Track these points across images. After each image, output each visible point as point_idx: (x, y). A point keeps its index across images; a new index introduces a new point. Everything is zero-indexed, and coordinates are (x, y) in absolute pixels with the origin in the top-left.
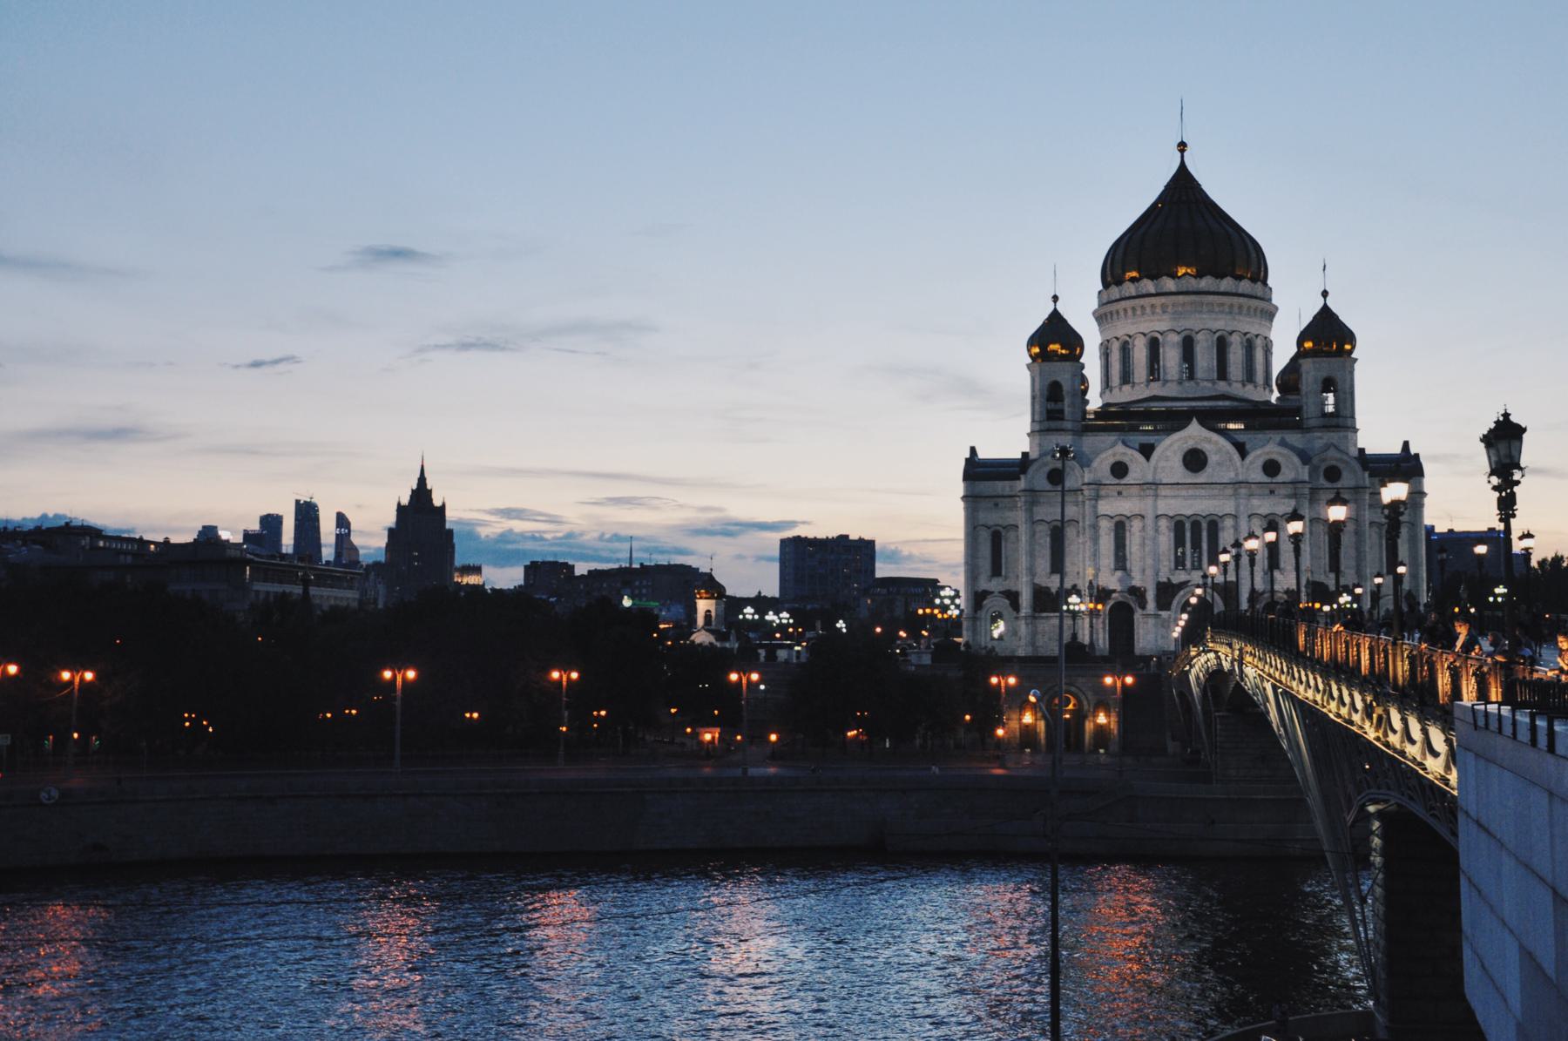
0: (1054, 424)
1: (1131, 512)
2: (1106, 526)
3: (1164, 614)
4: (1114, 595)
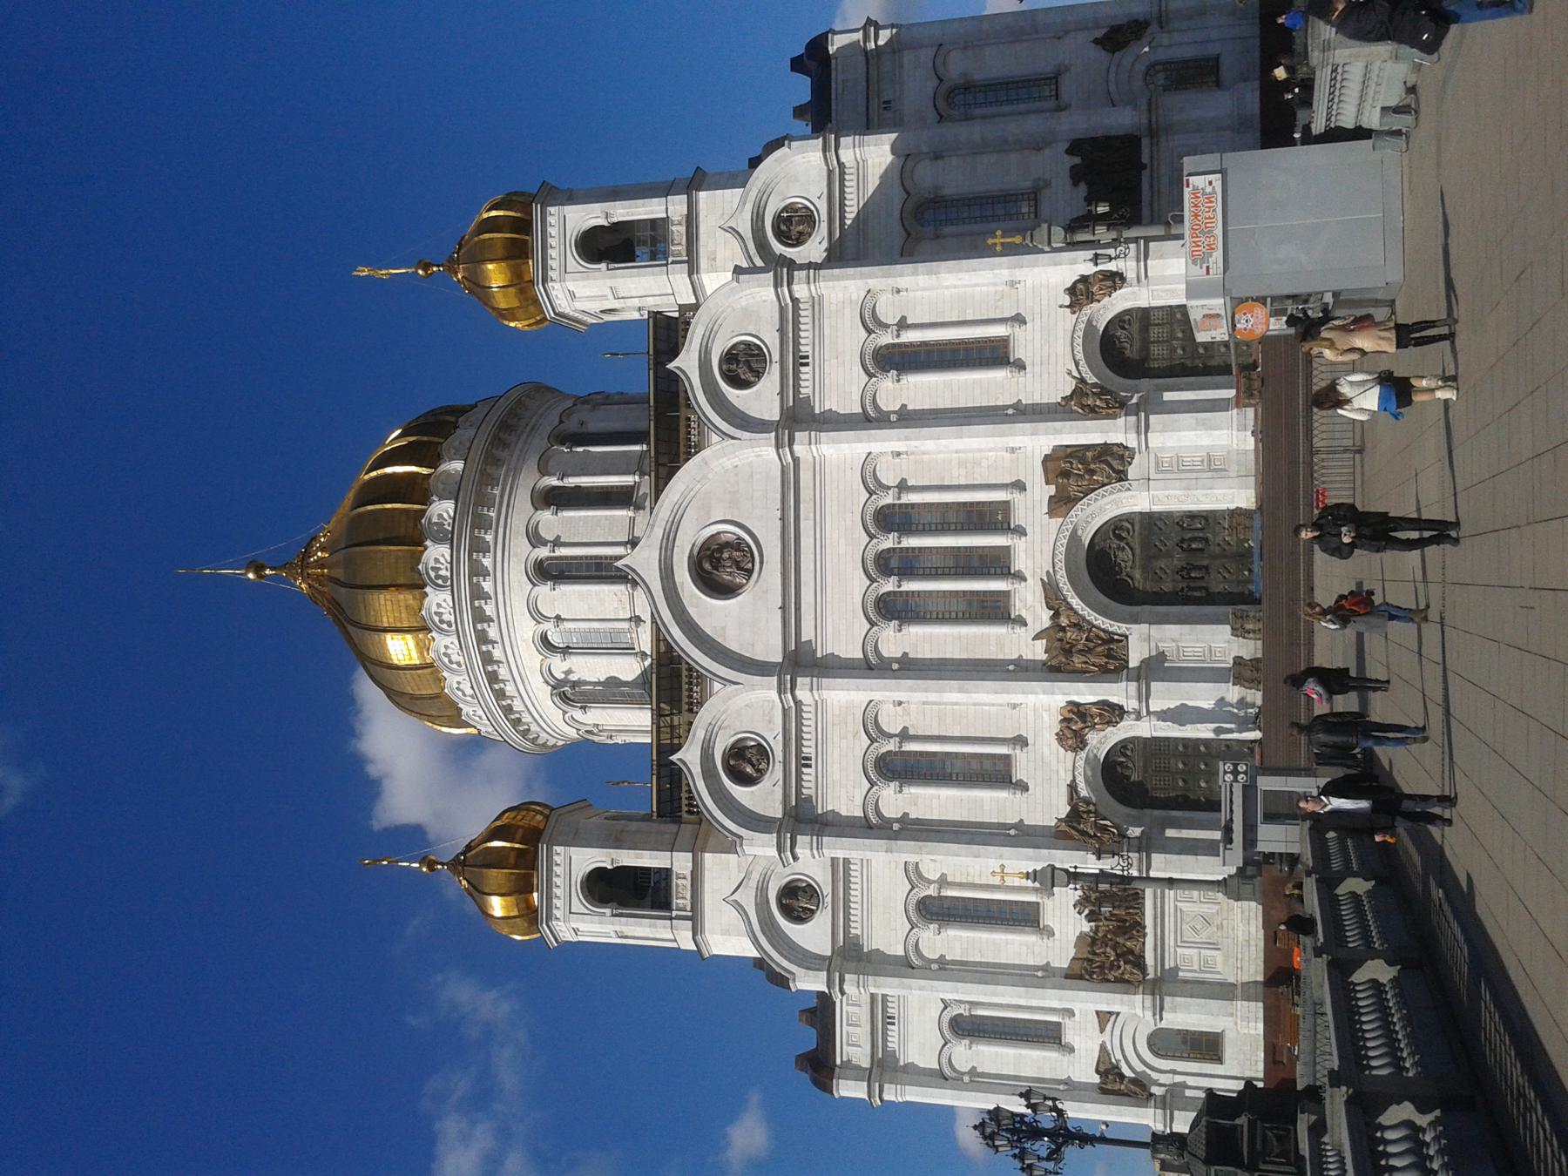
0: (681, 897)
1: (856, 734)
2: (896, 801)
3: (1136, 656)
4: (1084, 791)
